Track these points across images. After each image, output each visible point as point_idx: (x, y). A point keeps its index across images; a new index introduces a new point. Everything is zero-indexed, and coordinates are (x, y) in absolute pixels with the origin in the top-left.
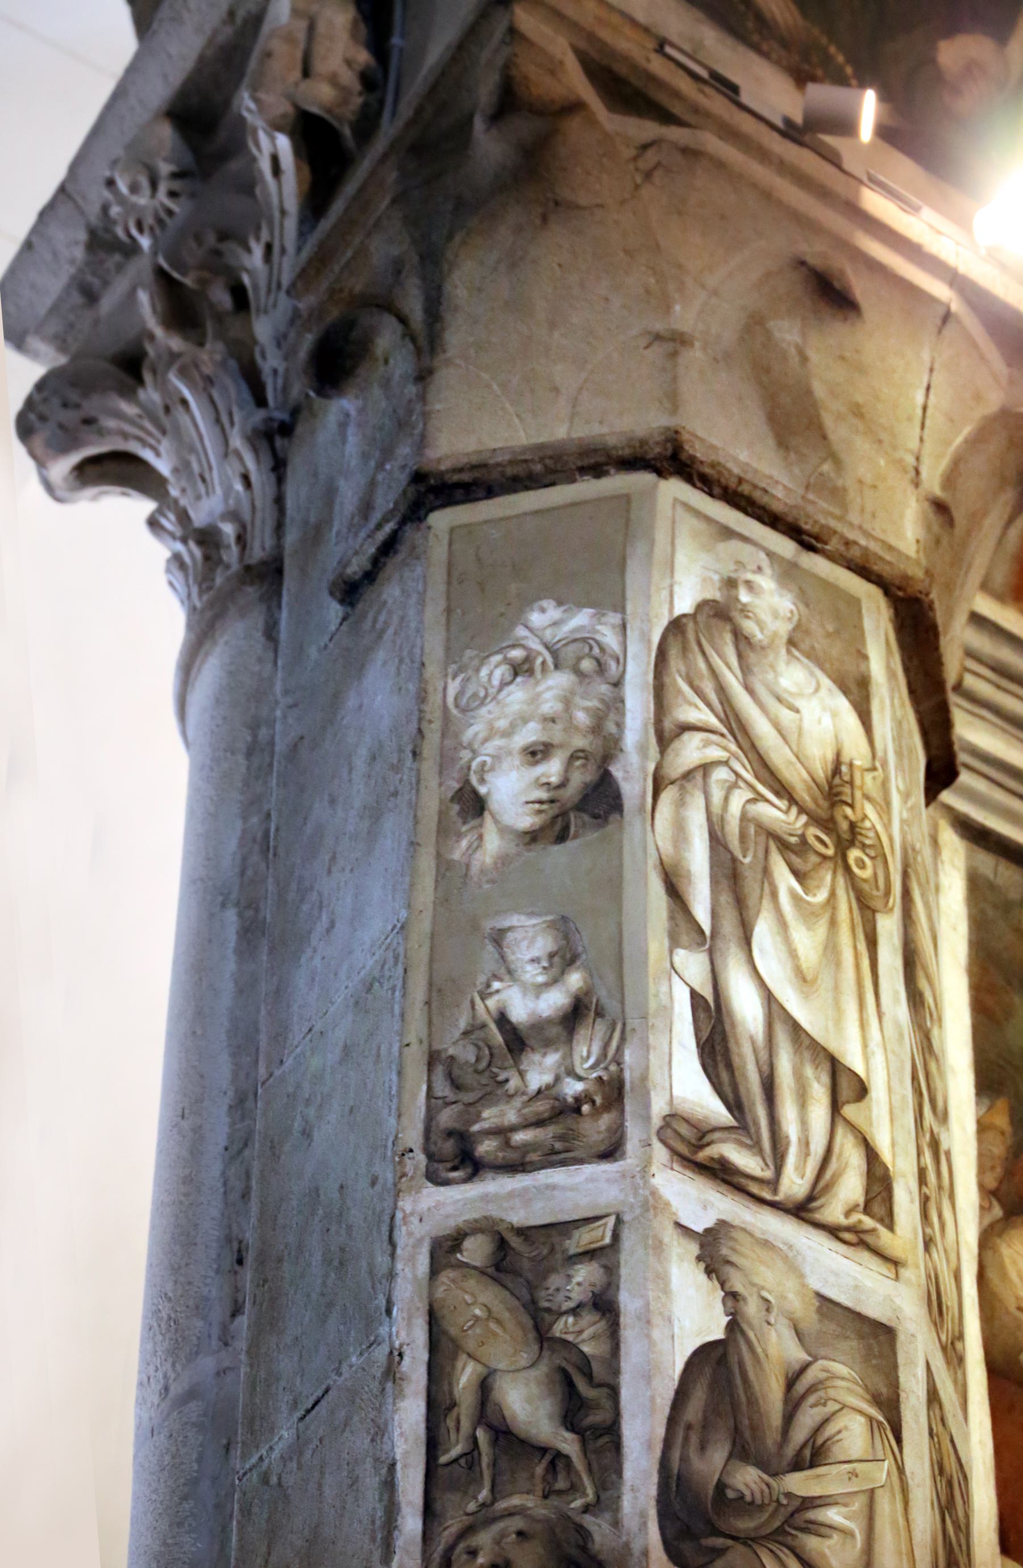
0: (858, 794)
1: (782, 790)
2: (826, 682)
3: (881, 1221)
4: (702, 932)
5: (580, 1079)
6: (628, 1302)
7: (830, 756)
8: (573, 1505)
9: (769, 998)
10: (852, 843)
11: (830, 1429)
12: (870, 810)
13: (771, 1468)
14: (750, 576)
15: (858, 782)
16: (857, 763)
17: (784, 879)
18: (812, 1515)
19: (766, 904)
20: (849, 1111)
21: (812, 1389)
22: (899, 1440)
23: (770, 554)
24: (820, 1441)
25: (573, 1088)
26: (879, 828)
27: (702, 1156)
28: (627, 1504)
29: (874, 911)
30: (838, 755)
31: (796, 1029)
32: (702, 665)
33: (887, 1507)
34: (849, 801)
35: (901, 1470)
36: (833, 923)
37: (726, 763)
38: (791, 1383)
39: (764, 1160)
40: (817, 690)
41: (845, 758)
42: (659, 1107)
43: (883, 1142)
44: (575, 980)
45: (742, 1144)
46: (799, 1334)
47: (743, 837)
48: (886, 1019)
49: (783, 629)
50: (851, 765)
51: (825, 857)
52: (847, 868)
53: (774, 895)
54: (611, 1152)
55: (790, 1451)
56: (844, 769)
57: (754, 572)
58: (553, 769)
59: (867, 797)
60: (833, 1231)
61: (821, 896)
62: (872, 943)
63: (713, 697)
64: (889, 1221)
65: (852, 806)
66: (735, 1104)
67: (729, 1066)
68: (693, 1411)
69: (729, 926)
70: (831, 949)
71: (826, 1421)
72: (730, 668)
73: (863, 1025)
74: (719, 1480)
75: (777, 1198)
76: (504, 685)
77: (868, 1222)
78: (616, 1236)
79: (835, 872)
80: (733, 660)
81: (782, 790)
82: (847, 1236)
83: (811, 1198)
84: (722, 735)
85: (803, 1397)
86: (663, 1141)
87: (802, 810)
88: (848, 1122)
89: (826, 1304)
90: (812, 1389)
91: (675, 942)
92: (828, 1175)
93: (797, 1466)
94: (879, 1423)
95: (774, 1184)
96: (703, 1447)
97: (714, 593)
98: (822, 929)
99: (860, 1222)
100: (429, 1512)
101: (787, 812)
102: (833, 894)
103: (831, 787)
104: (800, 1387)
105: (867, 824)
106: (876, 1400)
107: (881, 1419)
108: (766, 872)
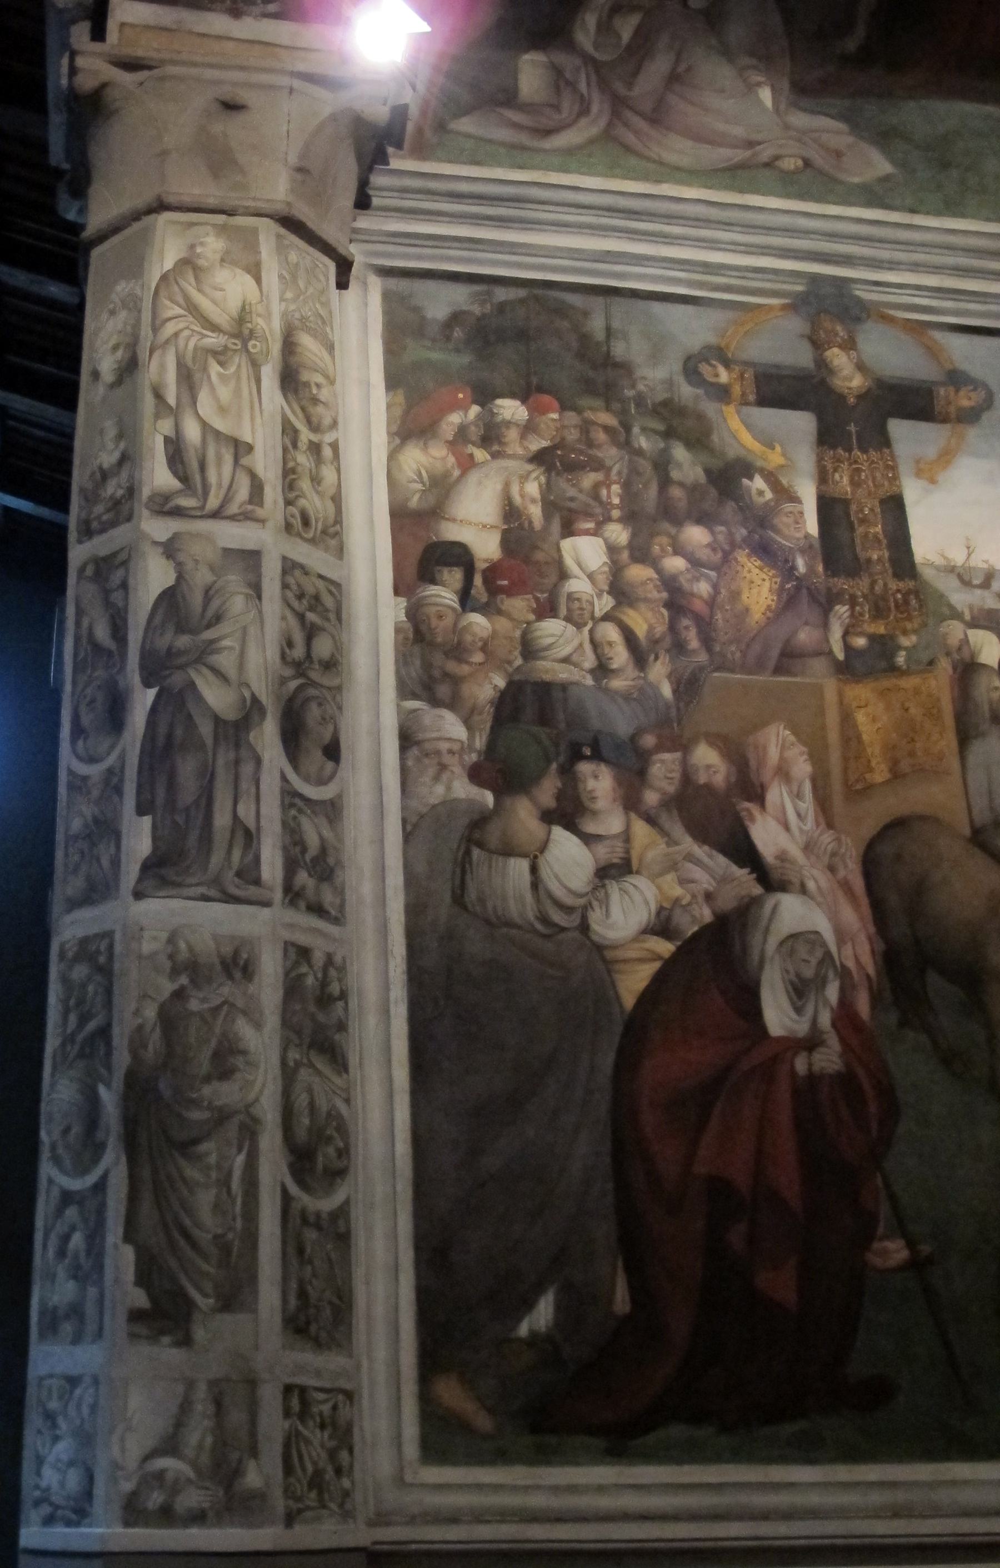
0: (254, 316)
1: (215, 328)
2: (238, 271)
3: (257, 505)
4: (170, 408)
5: (122, 488)
6: (131, 582)
7: (240, 304)
8: (114, 672)
9: (205, 426)
10: (250, 339)
11: (228, 604)
12: (260, 321)
13: (194, 632)
14: (202, 240)
15: (254, 310)
16: (252, 302)
17: (214, 368)
18: (214, 646)
19: (205, 383)
20: (244, 461)
21: (217, 592)
22: (259, 597)
23: (214, 225)
24: (221, 612)
25: (120, 492)
26: (264, 327)
27: (167, 508)
28: (129, 668)
29: (260, 366)
30: (244, 302)
31: (217, 434)
32: (176, 288)
33: (253, 630)
34: (250, 320)
35: (260, 612)
36: (239, 379)
37: (187, 328)
38: (207, 591)
39: (198, 498)
40: (235, 276)
41: (248, 302)
42: (146, 492)
43: (260, 470)
44: (122, 445)
45: (186, 496)
46: (212, 568)
47: (194, 358)
48: (266, 414)
49: (218, 257)
50: (250, 304)
51: (236, 351)
52: (247, 351)
53: (209, 377)
54: (129, 519)
55: (205, 622)
56: (247, 307)
57: (204, 237)
58: (119, 354)
59: (259, 315)
60: (233, 518)
61: (233, 369)
62: (258, 381)
63: (180, 299)
64: (261, 504)
65: (251, 322)
66: (184, 479)
67: (182, 462)
68: (158, 620)
69: (186, 399)
70: (237, 392)
71: (224, 603)
72: (190, 285)
73: (252, 419)
74: (169, 646)
75: (204, 513)
76: (107, 320)
77: (250, 507)
78: (129, 554)
79: (241, 356)
80: (192, 280)
81: (215, 328)
82: (241, 517)
83: (222, 506)
84: (185, 316)
85: (213, 596)
86: (147, 508)
87: (225, 333)
88: (242, 466)
89: (227, 551)
90: (217, 592)
91: (157, 416)
92: (231, 494)
93: (208, 626)
94: (251, 595)
95: (202, 508)
96: (161, 634)
97: (182, 255)
98: (233, 384)
99: (246, 508)
100: (74, 683)
101: (218, 338)
102: (239, 366)
103: (240, 318)
104: (211, 592)
105: (259, 327)
106: (250, 585)
107: (252, 592)
108: (205, 369)
